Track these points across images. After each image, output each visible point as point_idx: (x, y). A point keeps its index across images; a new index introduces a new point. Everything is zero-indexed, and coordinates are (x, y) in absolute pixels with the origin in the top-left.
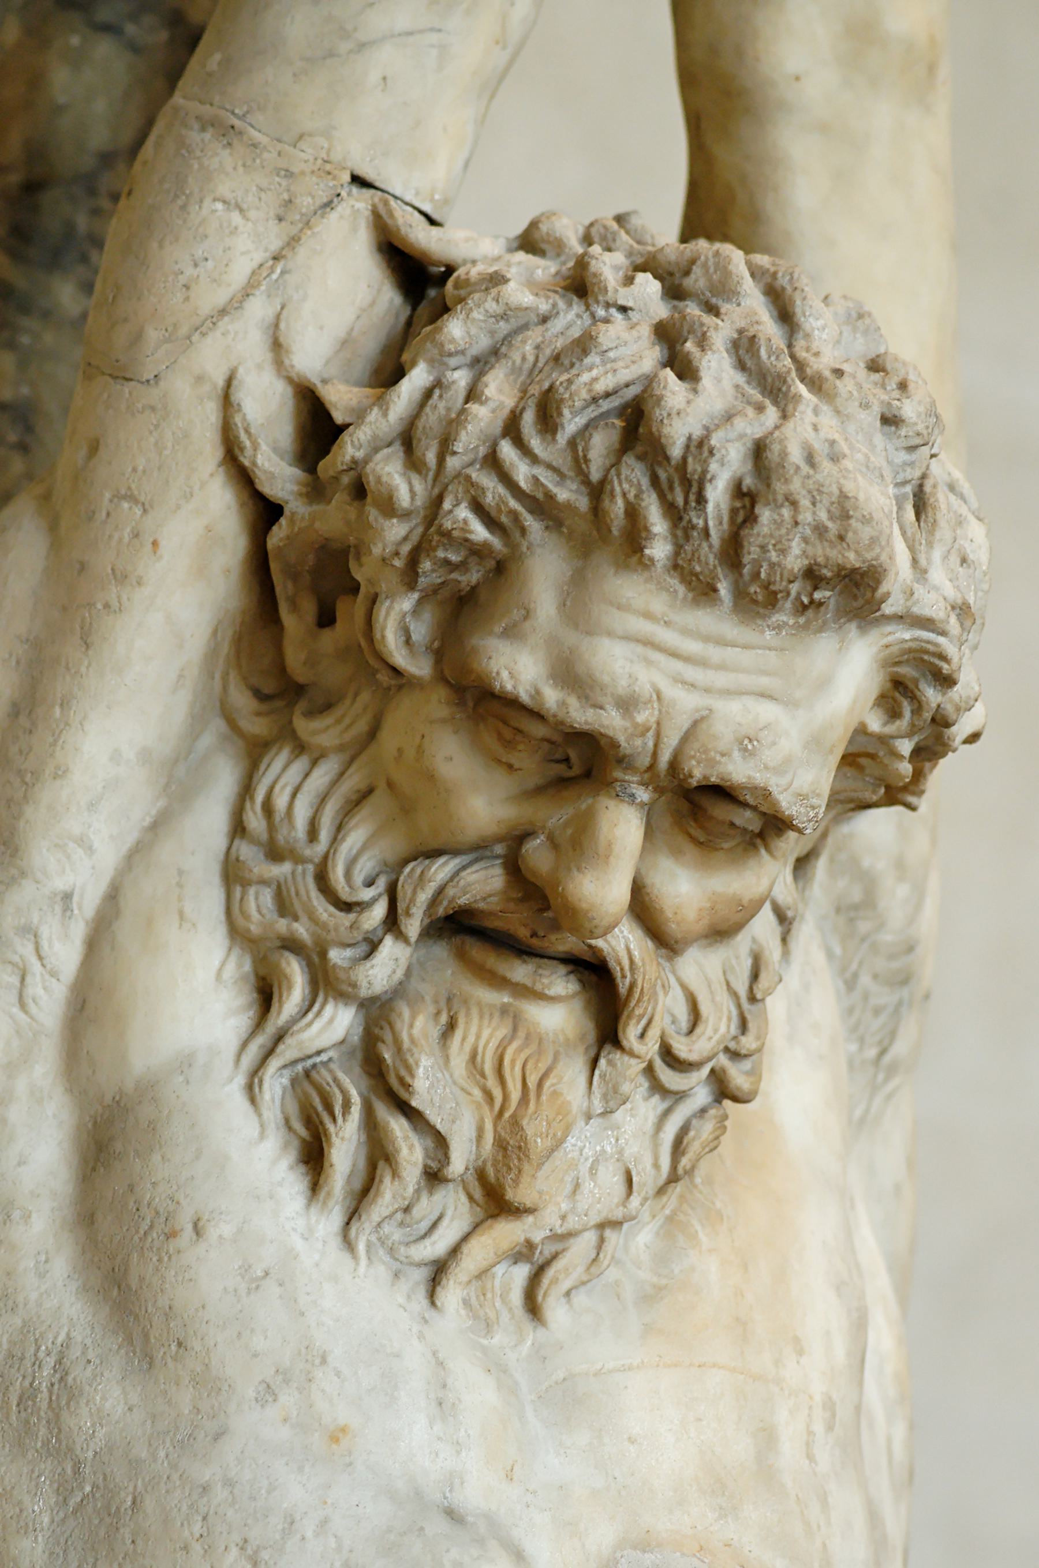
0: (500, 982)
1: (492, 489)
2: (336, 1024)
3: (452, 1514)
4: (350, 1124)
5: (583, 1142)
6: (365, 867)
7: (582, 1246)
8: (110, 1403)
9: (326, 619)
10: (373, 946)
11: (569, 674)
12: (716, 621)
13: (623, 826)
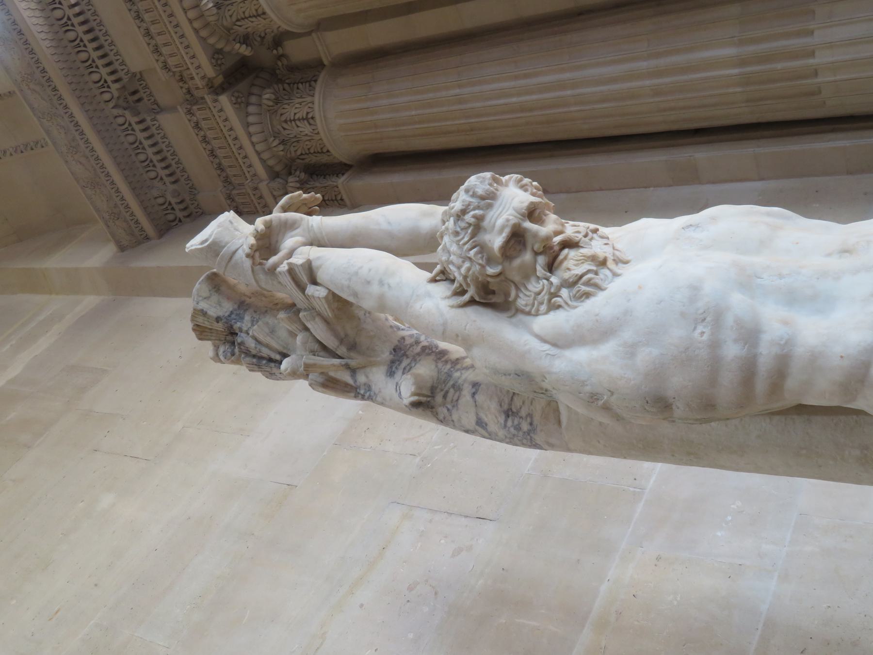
0: (562, 262)
1: (466, 247)
2: (564, 292)
4: (583, 288)
6: (538, 286)
7: (617, 253)
8: (627, 335)
9: (493, 292)
10: (552, 283)
12: (497, 204)
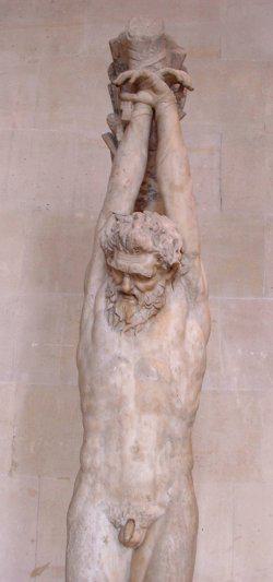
8: (91, 349)
11: (117, 264)
13: (127, 280)
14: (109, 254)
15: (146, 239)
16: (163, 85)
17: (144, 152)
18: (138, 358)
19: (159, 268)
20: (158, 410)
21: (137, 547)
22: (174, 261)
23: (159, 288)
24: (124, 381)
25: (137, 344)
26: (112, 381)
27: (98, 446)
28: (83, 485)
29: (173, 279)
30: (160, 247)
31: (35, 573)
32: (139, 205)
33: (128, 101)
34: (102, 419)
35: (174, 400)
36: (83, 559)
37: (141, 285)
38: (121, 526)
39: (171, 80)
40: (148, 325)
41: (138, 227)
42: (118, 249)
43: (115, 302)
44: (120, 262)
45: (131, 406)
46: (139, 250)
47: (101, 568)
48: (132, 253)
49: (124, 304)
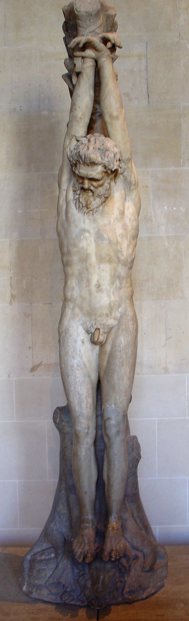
3: (84, 230)
5: (93, 203)
8: (66, 225)
11: (79, 172)
13: (86, 182)
14: (74, 165)
15: (96, 156)
16: (101, 46)
17: (92, 93)
18: (96, 230)
19: (106, 172)
20: (110, 261)
21: (102, 345)
22: (115, 168)
23: (106, 184)
24: (88, 244)
25: (95, 221)
26: (81, 245)
27: (74, 285)
28: (67, 310)
29: (115, 176)
30: (106, 161)
31: (33, 369)
32: (90, 129)
33: (78, 57)
34: (75, 269)
35: (120, 255)
36: (70, 353)
37: (95, 184)
38: (91, 333)
39: (105, 41)
40: (101, 208)
41: (91, 148)
42: (80, 162)
43: (79, 195)
44: (81, 171)
45: (93, 259)
46: (93, 164)
47: (81, 358)
48: (88, 165)
49: (85, 196)
